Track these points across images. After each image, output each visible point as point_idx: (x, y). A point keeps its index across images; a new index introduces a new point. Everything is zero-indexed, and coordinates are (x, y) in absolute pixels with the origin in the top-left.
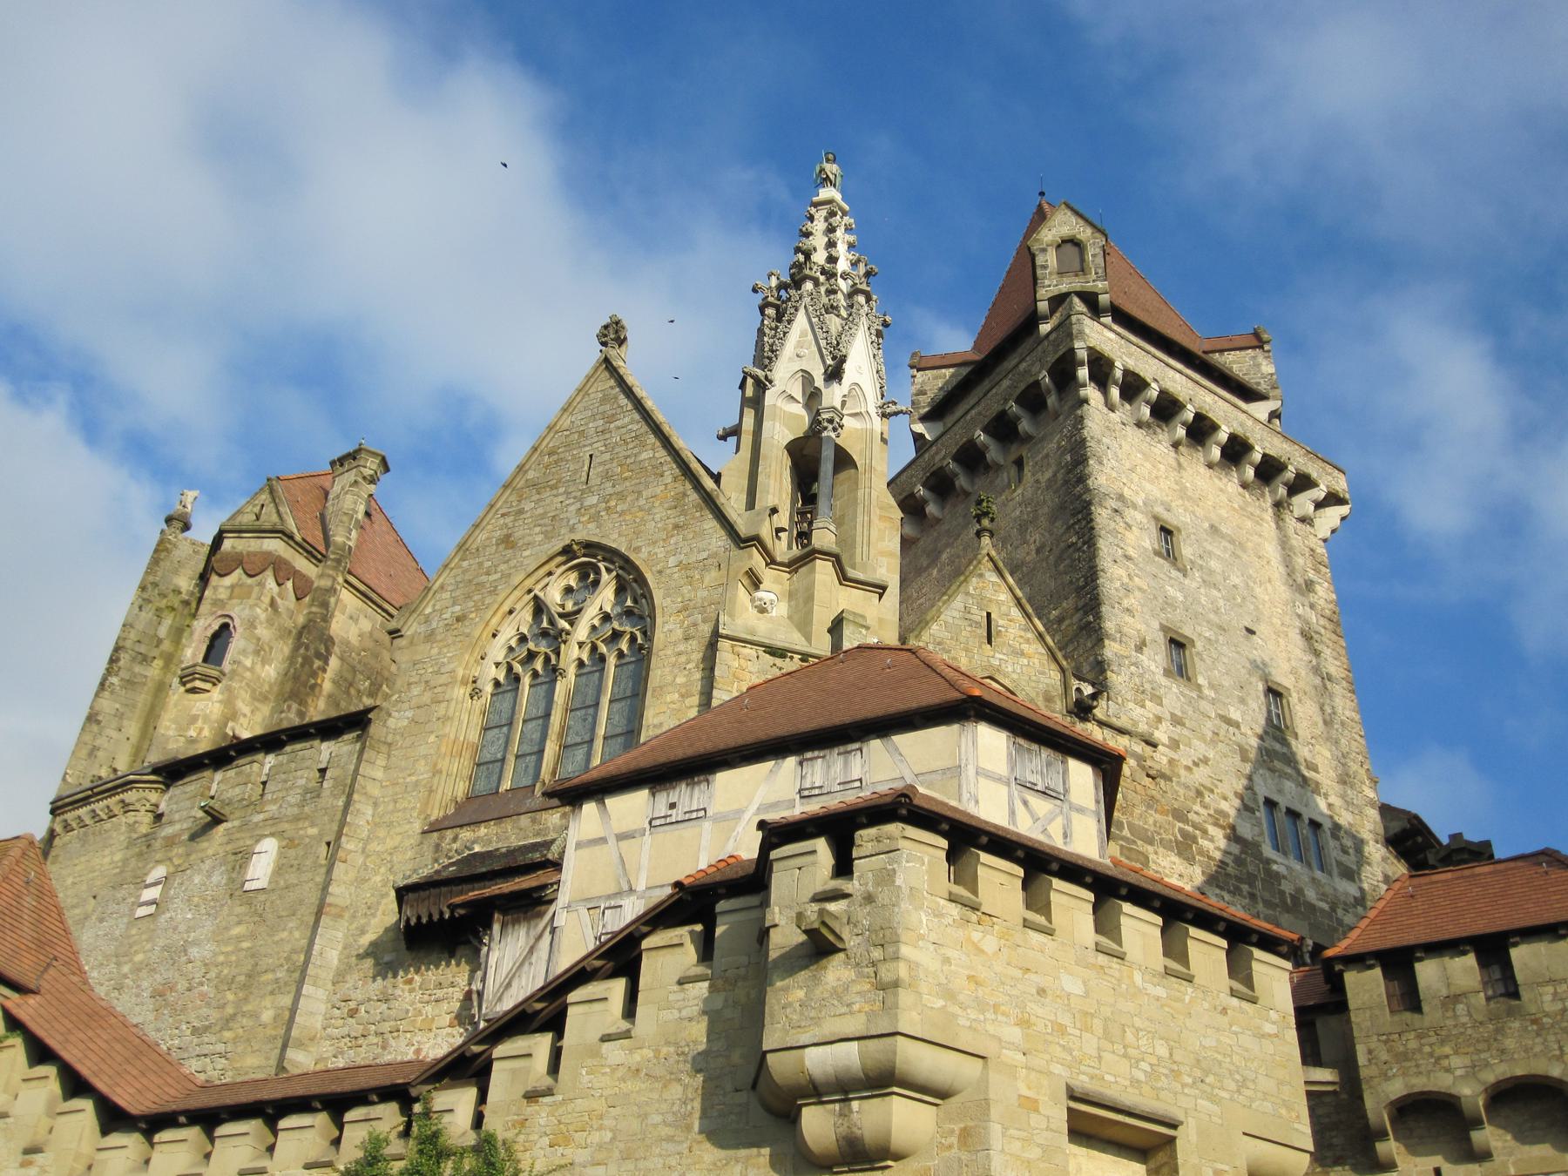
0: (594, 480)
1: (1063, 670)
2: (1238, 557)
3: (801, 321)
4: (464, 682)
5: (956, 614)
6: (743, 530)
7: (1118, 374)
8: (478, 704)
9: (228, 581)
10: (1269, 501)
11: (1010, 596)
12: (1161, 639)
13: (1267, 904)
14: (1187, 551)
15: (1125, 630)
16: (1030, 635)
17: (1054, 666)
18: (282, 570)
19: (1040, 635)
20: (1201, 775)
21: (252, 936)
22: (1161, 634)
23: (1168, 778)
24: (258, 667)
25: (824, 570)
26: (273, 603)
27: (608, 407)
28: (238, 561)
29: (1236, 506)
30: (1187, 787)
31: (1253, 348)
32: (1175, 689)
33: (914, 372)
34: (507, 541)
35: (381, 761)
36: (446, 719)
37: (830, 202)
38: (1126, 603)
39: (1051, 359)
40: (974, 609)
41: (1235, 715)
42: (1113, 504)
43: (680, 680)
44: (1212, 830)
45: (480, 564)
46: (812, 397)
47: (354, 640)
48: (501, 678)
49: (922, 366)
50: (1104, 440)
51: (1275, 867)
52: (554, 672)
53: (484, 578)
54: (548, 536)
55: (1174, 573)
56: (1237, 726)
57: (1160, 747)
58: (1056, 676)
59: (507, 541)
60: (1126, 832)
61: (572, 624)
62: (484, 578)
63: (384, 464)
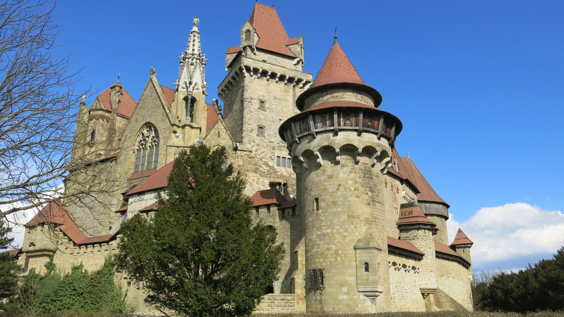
0: (150, 108)
1: (233, 141)
2: (281, 103)
3: (185, 69)
4: (132, 150)
5: (213, 133)
6: (172, 123)
7: (252, 69)
8: (135, 154)
9: (93, 121)
10: (292, 85)
11: (223, 127)
12: (257, 128)
13: (273, 178)
14: (267, 105)
15: (249, 129)
16: (227, 135)
17: (231, 140)
18: (103, 117)
19: (229, 135)
20: (262, 155)
21: (104, 199)
22: (257, 127)
23: (254, 158)
24: (102, 139)
25: (187, 128)
26: (102, 125)
27: (151, 90)
28: (94, 117)
29: (282, 90)
30: (258, 158)
31: (296, 44)
32: (259, 138)
33: (226, 55)
34: (137, 121)
35: (120, 166)
36: (129, 158)
37: (195, 31)
38: (249, 123)
39: (239, 67)
40: (216, 131)
41: (273, 140)
42: (249, 100)
43: (163, 153)
44: (263, 166)
45: (133, 125)
46: (187, 88)
47: (121, 126)
48: (138, 149)
49: (229, 53)
50: (249, 85)
51: (277, 170)
52: (145, 149)
53: (133, 128)
54: (143, 120)
55: (263, 112)
56: (273, 142)
57: (253, 152)
58: (231, 142)
59: (137, 121)
60: (243, 171)
61: (148, 138)
62: (133, 128)
63: (121, 88)
